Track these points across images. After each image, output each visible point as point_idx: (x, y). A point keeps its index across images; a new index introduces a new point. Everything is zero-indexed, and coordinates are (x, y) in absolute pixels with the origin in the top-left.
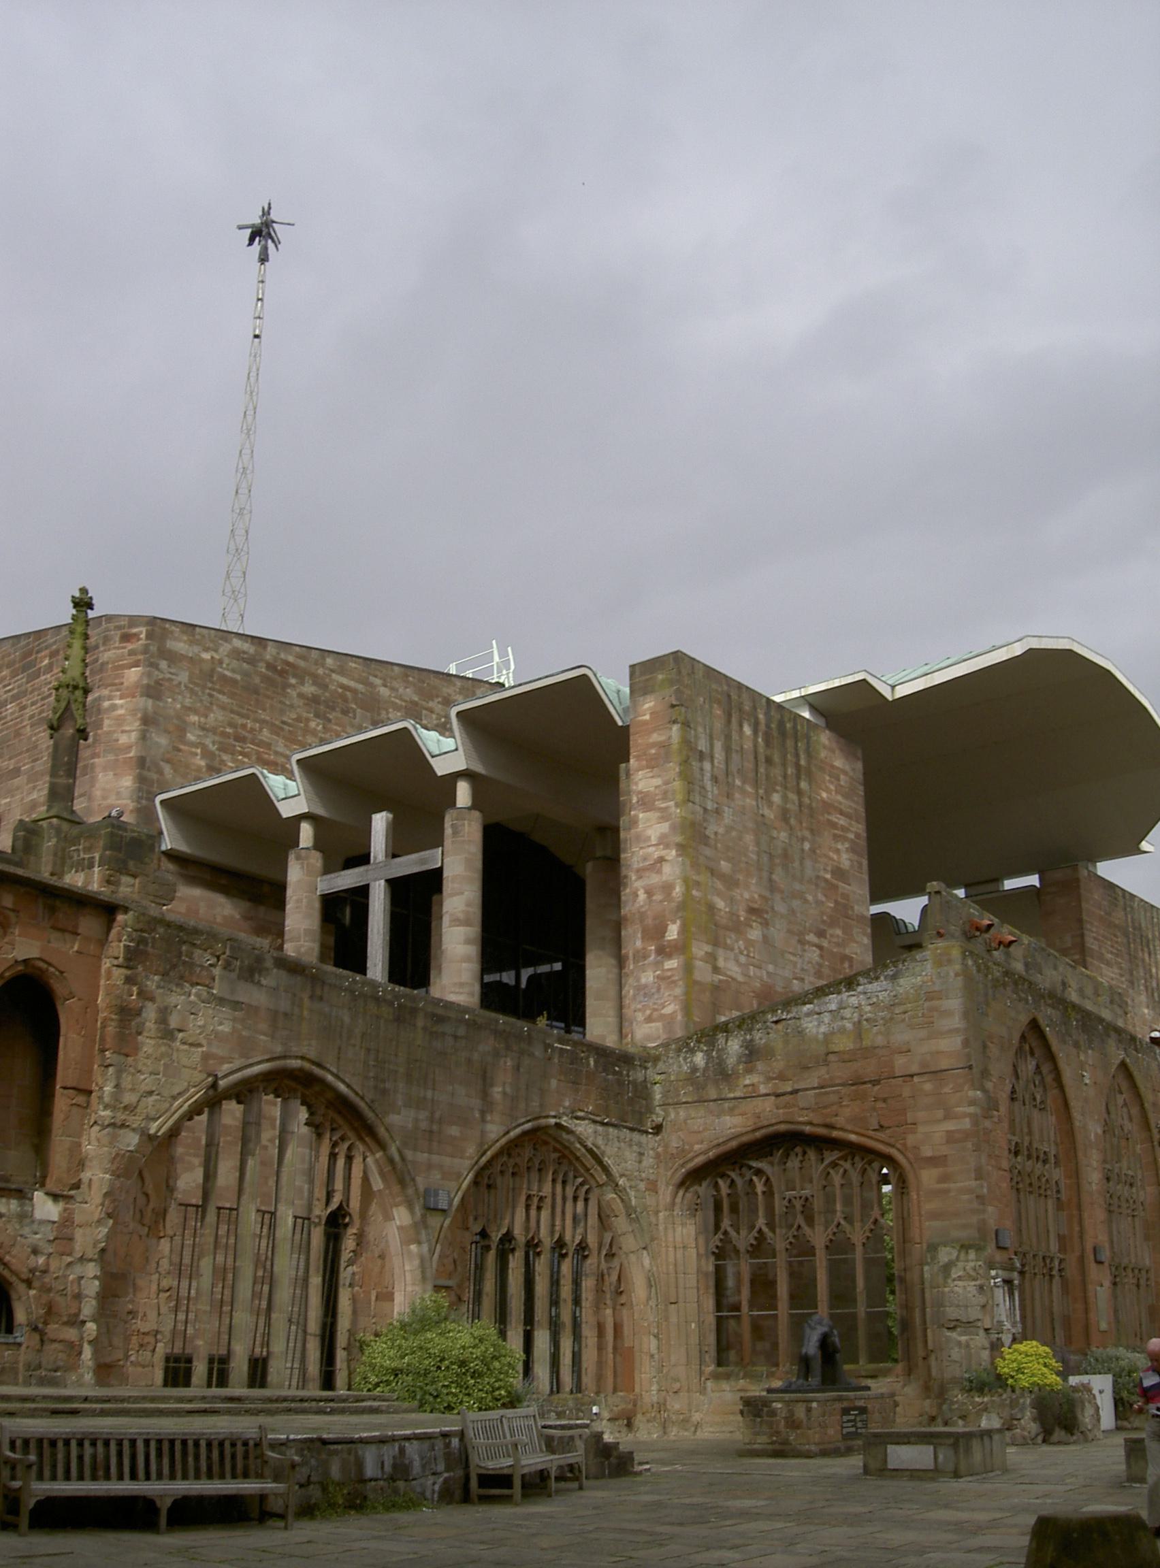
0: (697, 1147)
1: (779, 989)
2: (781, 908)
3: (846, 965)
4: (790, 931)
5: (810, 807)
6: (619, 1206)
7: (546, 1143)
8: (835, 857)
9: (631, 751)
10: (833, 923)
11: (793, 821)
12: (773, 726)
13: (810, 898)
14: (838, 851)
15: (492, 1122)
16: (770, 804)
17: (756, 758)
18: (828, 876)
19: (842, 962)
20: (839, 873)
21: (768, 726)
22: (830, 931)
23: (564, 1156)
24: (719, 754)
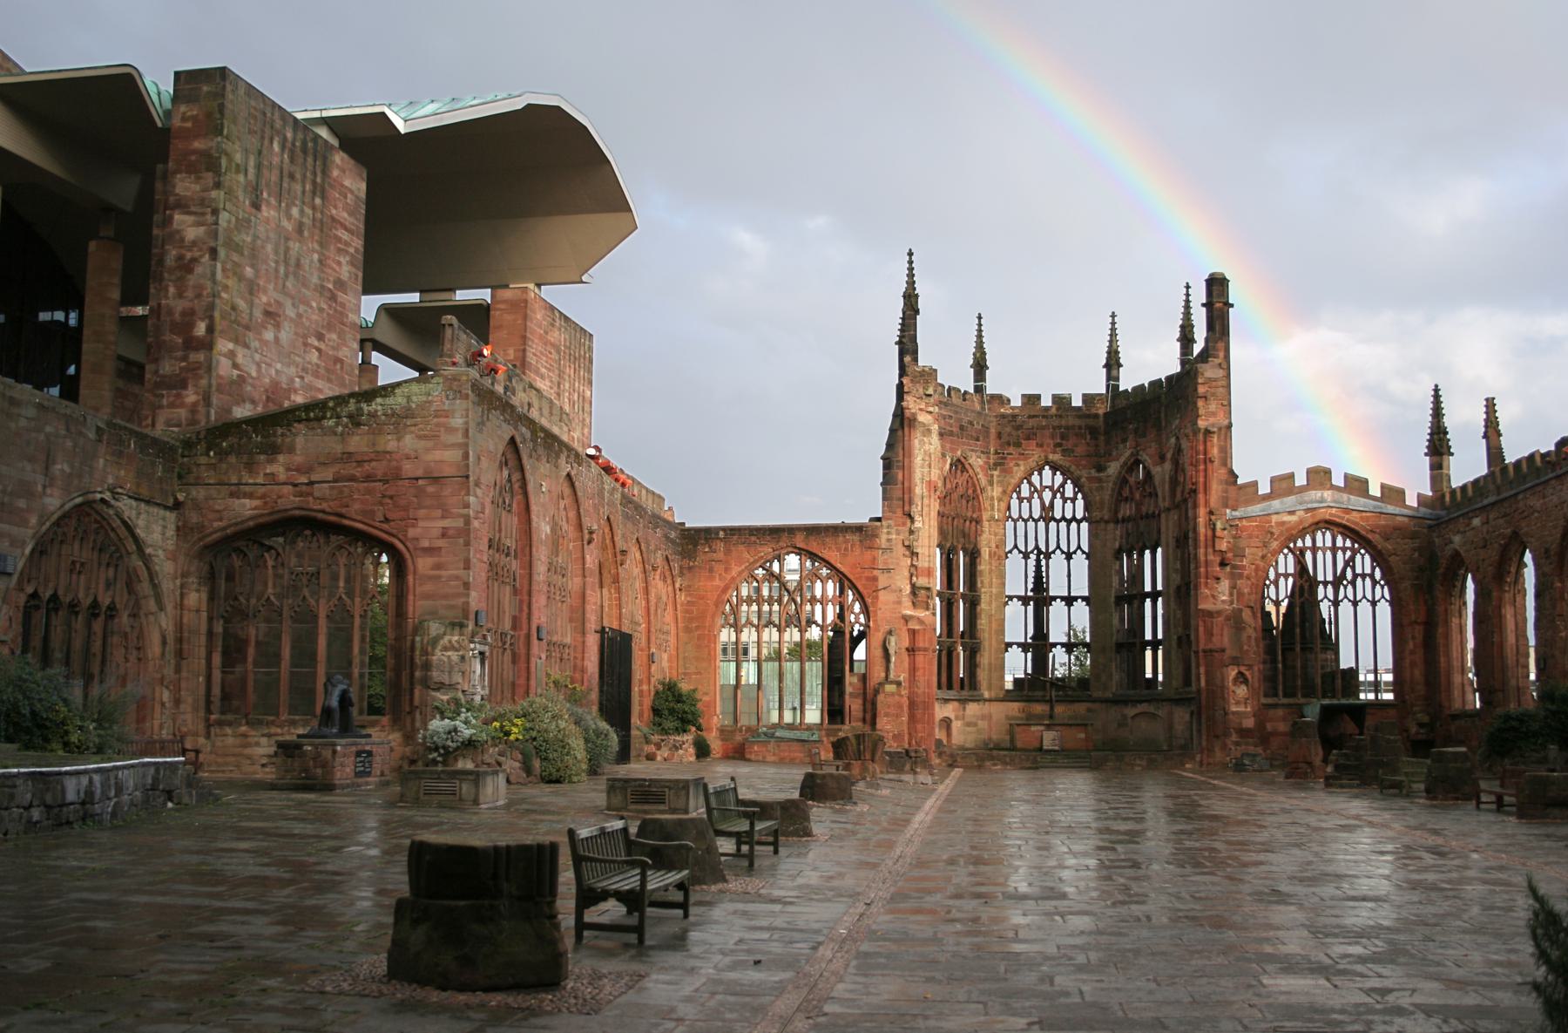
0: (216, 524)
1: (284, 386)
2: (291, 312)
3: (338, 366)
4: (296, 334)
5: (321, 221)
6: (144, 574)
7: (89, 515)
8: (337, 268)
9: (171, 153)
10: (330, 327)
11: (306, 233)
12: (298, 144)
13: (314, 304)
14: (339, 263)
15: (51, 496)
16: (289, 217)
17: (281, 172)
18: (331, 286)
19: (335, 363)
20: (340, 284)
21: (294, 145)
22: (328, 336)
23: (102, 527)
24: (251, 171)
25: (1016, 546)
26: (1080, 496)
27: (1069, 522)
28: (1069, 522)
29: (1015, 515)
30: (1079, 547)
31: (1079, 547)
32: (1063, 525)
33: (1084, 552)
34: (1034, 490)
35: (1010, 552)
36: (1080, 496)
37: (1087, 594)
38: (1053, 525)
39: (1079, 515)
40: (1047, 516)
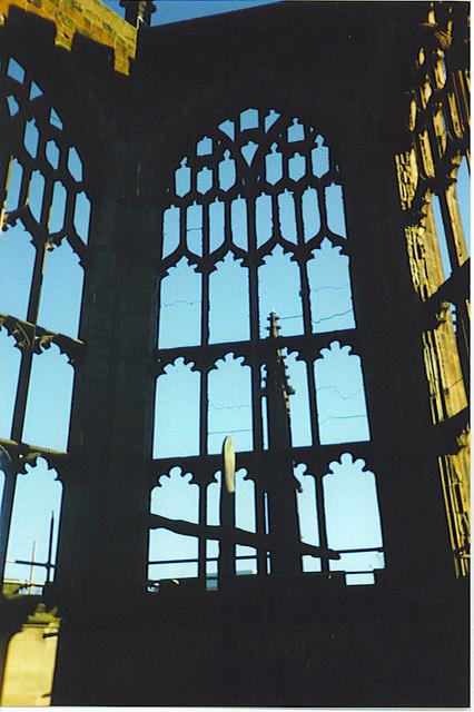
25: (182, 249)
26: (320, 140)
27: (298, 190)
28: (298, 190)
29: (182, 188)
30: (324, 231)
31: (324, 231)
32: (286, 199)
33: (336, 240)
34: (221, 143)
35: (173, 260)
36: (320, 140)
37: (349, 323)
38: (264, 202)
39: (321, 166)
40: (251, 183)
